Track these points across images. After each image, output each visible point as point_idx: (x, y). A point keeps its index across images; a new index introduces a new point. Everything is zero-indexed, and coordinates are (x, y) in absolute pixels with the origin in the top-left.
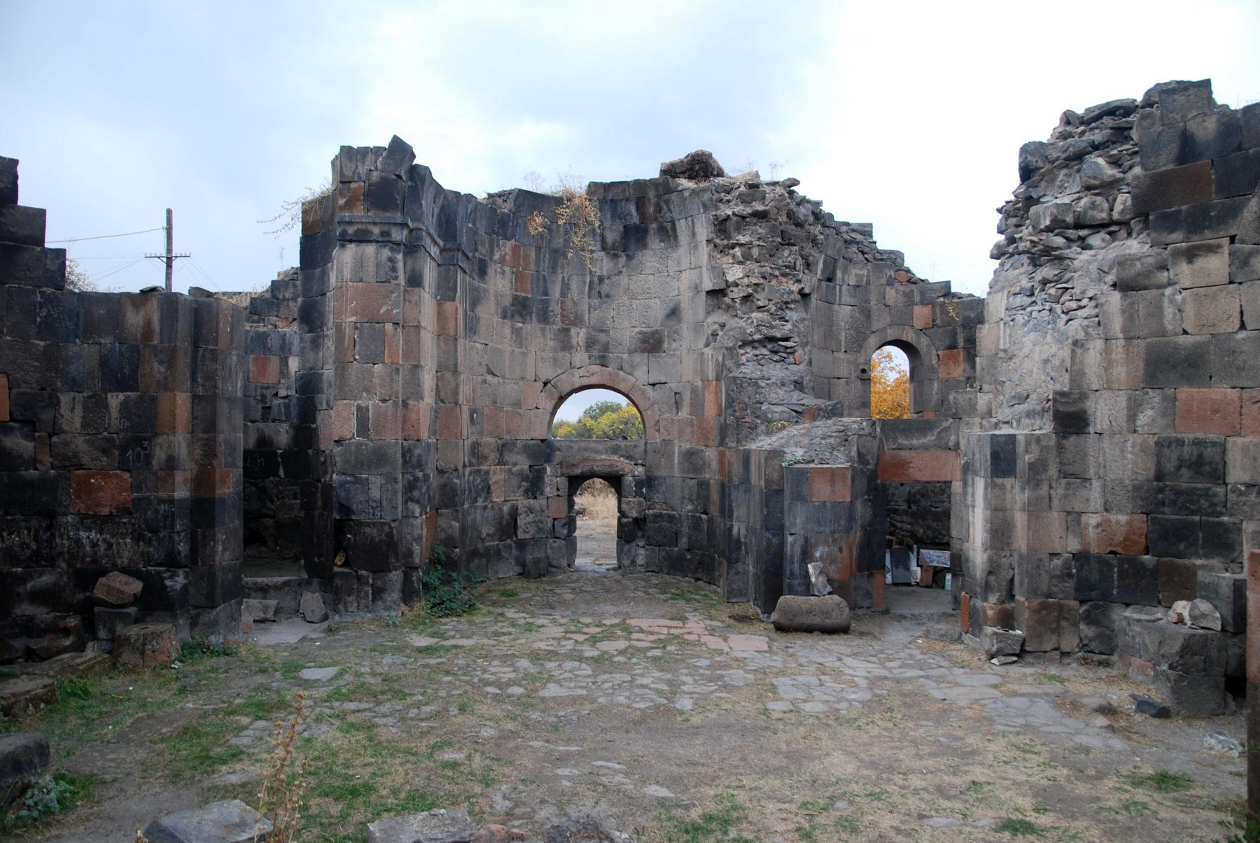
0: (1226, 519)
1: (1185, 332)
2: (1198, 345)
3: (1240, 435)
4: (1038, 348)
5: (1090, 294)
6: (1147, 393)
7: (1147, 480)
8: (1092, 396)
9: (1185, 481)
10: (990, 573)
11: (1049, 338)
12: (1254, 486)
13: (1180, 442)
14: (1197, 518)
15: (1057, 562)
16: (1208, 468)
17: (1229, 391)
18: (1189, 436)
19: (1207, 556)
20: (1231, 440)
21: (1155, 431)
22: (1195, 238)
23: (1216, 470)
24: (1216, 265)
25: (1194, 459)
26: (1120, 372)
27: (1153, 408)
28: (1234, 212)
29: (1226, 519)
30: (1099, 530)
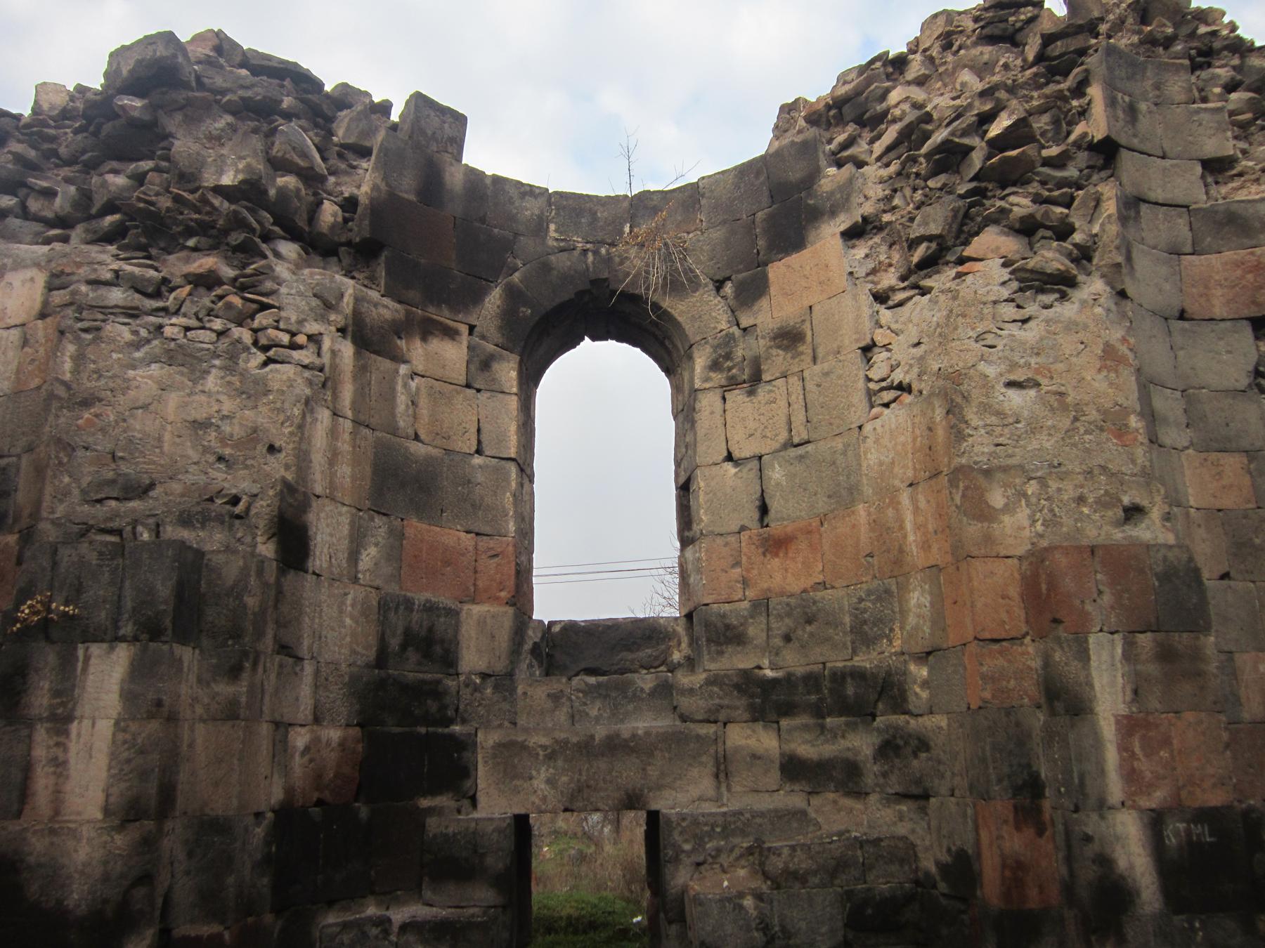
0: (457, 728)
1: (417, 437)
2: (429, 460)
3: (473, 601)
4: (173, 399)
5: (313, 327)
6: (372, 519)
7: (368, 666)
8: (315, 504)
9: (411, 671)
10: (146, 879)
11: (212, 382)
12: (490, 676)
13: (409, 603)
14: (423, 730)
15: (260, 831)
16: (438, 649)
17: (463, 535)
18: (421, 597)
19: (433, 792)
20: (466, 607)
21: (378, 582)
22: (431, 309)
23: (447, 651)
24: (452, 355)
25: (423, 633)
26: (345, 471)
27: (376, 545)
28: (475, 297)
29: (457, 728)
30: (307, 758)
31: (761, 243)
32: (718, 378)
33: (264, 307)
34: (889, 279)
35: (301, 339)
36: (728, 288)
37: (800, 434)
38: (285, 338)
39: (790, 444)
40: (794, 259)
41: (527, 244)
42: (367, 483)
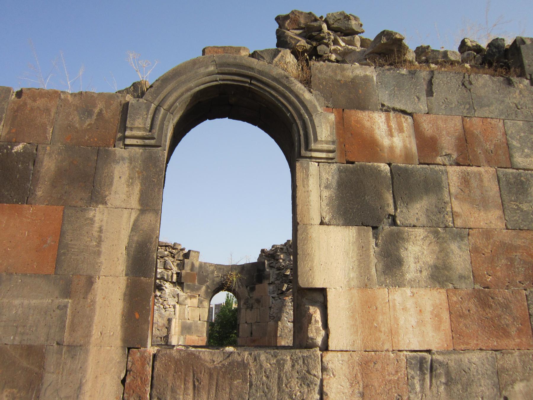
2: (191, 324)
24: (195, 301)
26: (177, 329)
31: (255, 280)
32: (245, 306)
33: (165, 300)
34: (275, 295)
35: (171, 306)
36: (248, 288)
37: (259, 321)
38: (168, 306)
39: (257, 322)
40: (260, 285)
41: (210, 275)
42: (180, 330)
